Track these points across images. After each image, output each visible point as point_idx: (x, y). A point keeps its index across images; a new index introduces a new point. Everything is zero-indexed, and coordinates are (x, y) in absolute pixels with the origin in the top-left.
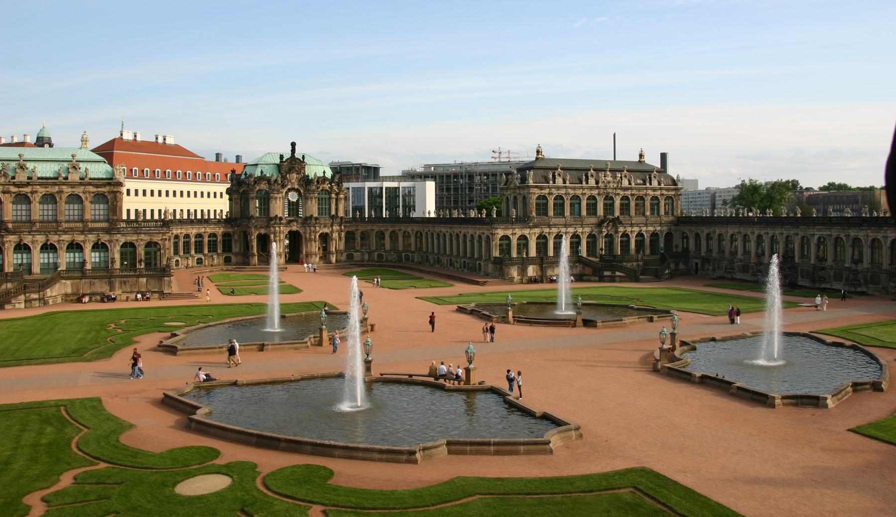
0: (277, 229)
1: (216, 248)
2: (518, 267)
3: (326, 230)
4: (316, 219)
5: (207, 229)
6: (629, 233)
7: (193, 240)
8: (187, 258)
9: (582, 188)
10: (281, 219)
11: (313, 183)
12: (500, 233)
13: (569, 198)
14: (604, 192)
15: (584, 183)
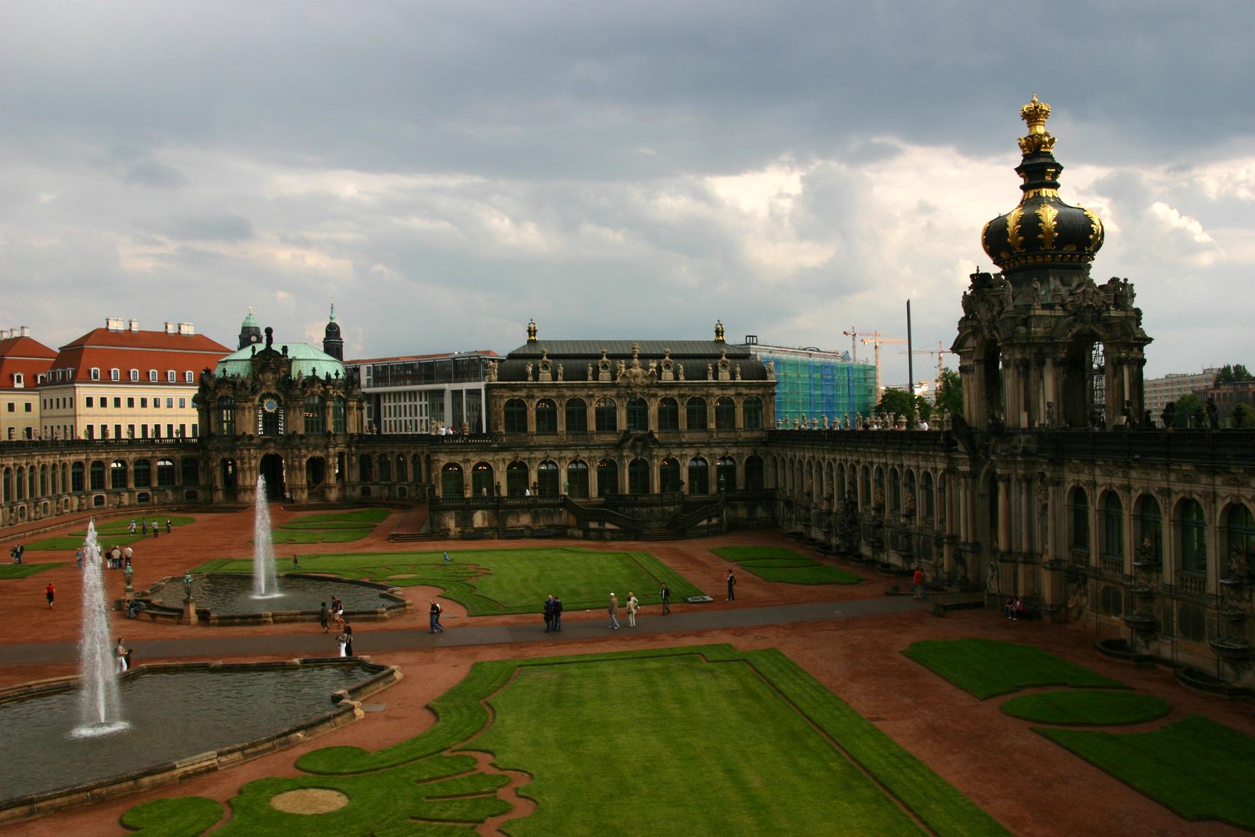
0: (245, 452)
1: (174, 480)
2: (457, 514)
3: (318, 454)
4: (302, 437)
5: (157, 452)
6: (678, 459)
7: (131, 468)
8: (119, 494)
9: (589, 387)
10: (251, 437)
11: (297, 386)
12: (444, 459)
13: (564, 404)
14: (628, 393)
15: (590, 377)
